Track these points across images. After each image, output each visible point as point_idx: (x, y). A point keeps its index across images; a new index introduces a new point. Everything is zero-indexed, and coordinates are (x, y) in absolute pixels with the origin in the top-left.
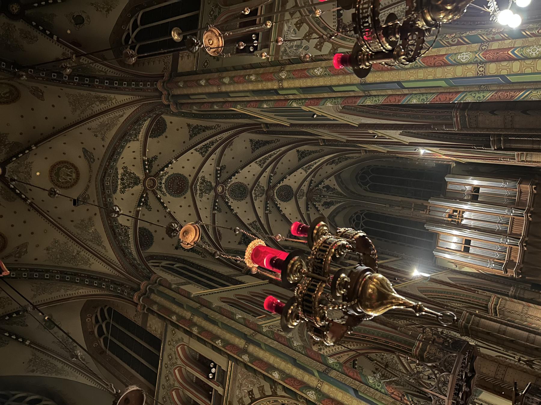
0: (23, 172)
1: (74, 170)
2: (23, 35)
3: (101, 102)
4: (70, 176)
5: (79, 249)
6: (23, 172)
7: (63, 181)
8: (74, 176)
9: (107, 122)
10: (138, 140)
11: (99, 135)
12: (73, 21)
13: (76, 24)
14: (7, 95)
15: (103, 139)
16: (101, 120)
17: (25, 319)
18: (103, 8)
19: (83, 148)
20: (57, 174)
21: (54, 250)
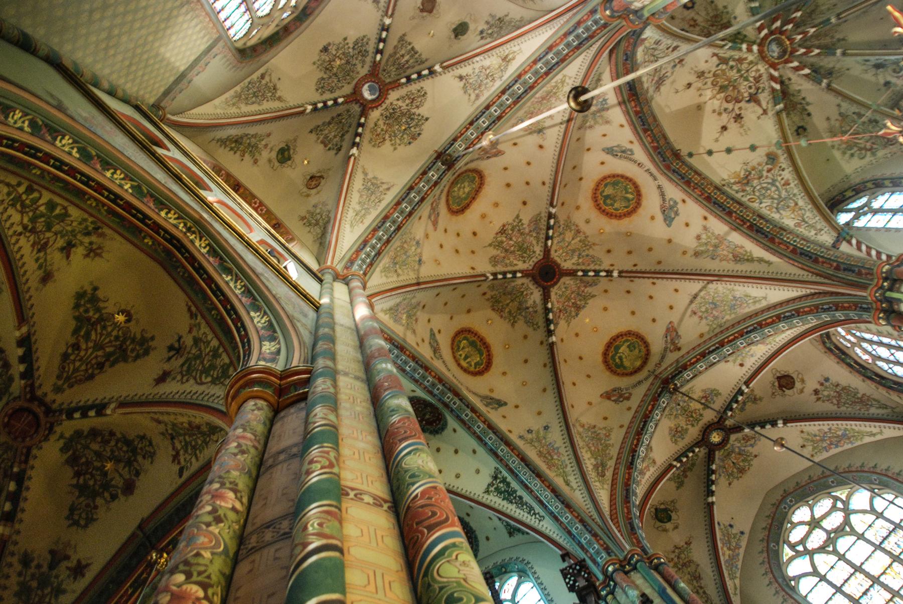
0: (508, 305)
1: (472, 369)
2: (680, 429)
3: (596, 467)
4: (466, 358)
5: (401, 278)
6: (508, 305)
7: (462, 345)
8: (464, 364)
9: (555, 457)
10: (487, 491)
11: (530, 436)
12: (662, 507)
13: (656, 509)
14: (617, 360)
15: (520, 437)
16: (562, 450)
17: (318, 139)
18: (678, 558)
19: (505, 404)
20: (472, 344)
21: (413, 248)
